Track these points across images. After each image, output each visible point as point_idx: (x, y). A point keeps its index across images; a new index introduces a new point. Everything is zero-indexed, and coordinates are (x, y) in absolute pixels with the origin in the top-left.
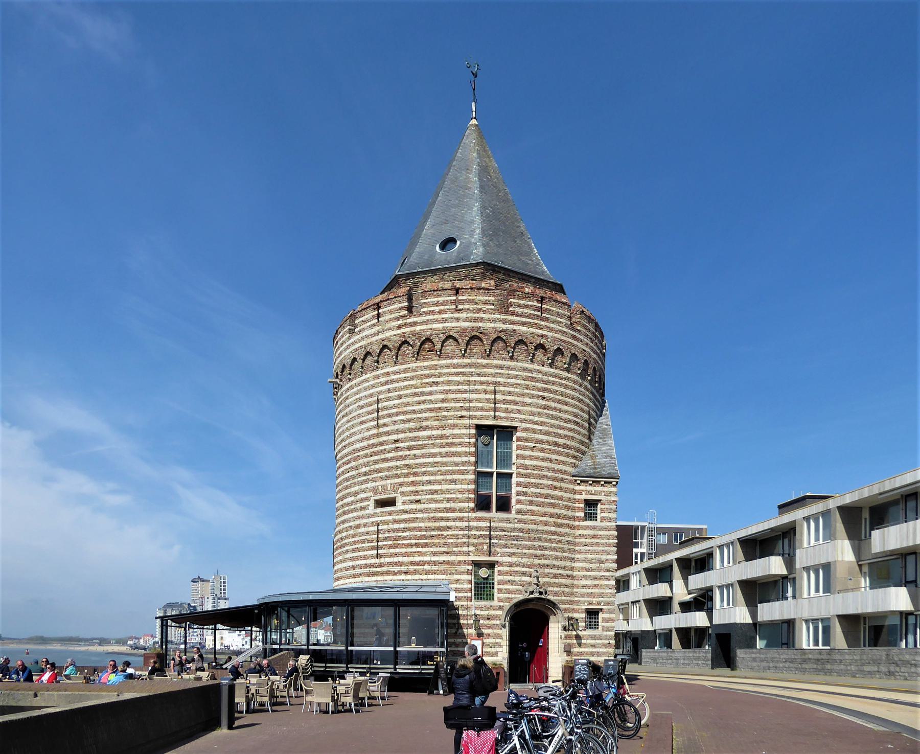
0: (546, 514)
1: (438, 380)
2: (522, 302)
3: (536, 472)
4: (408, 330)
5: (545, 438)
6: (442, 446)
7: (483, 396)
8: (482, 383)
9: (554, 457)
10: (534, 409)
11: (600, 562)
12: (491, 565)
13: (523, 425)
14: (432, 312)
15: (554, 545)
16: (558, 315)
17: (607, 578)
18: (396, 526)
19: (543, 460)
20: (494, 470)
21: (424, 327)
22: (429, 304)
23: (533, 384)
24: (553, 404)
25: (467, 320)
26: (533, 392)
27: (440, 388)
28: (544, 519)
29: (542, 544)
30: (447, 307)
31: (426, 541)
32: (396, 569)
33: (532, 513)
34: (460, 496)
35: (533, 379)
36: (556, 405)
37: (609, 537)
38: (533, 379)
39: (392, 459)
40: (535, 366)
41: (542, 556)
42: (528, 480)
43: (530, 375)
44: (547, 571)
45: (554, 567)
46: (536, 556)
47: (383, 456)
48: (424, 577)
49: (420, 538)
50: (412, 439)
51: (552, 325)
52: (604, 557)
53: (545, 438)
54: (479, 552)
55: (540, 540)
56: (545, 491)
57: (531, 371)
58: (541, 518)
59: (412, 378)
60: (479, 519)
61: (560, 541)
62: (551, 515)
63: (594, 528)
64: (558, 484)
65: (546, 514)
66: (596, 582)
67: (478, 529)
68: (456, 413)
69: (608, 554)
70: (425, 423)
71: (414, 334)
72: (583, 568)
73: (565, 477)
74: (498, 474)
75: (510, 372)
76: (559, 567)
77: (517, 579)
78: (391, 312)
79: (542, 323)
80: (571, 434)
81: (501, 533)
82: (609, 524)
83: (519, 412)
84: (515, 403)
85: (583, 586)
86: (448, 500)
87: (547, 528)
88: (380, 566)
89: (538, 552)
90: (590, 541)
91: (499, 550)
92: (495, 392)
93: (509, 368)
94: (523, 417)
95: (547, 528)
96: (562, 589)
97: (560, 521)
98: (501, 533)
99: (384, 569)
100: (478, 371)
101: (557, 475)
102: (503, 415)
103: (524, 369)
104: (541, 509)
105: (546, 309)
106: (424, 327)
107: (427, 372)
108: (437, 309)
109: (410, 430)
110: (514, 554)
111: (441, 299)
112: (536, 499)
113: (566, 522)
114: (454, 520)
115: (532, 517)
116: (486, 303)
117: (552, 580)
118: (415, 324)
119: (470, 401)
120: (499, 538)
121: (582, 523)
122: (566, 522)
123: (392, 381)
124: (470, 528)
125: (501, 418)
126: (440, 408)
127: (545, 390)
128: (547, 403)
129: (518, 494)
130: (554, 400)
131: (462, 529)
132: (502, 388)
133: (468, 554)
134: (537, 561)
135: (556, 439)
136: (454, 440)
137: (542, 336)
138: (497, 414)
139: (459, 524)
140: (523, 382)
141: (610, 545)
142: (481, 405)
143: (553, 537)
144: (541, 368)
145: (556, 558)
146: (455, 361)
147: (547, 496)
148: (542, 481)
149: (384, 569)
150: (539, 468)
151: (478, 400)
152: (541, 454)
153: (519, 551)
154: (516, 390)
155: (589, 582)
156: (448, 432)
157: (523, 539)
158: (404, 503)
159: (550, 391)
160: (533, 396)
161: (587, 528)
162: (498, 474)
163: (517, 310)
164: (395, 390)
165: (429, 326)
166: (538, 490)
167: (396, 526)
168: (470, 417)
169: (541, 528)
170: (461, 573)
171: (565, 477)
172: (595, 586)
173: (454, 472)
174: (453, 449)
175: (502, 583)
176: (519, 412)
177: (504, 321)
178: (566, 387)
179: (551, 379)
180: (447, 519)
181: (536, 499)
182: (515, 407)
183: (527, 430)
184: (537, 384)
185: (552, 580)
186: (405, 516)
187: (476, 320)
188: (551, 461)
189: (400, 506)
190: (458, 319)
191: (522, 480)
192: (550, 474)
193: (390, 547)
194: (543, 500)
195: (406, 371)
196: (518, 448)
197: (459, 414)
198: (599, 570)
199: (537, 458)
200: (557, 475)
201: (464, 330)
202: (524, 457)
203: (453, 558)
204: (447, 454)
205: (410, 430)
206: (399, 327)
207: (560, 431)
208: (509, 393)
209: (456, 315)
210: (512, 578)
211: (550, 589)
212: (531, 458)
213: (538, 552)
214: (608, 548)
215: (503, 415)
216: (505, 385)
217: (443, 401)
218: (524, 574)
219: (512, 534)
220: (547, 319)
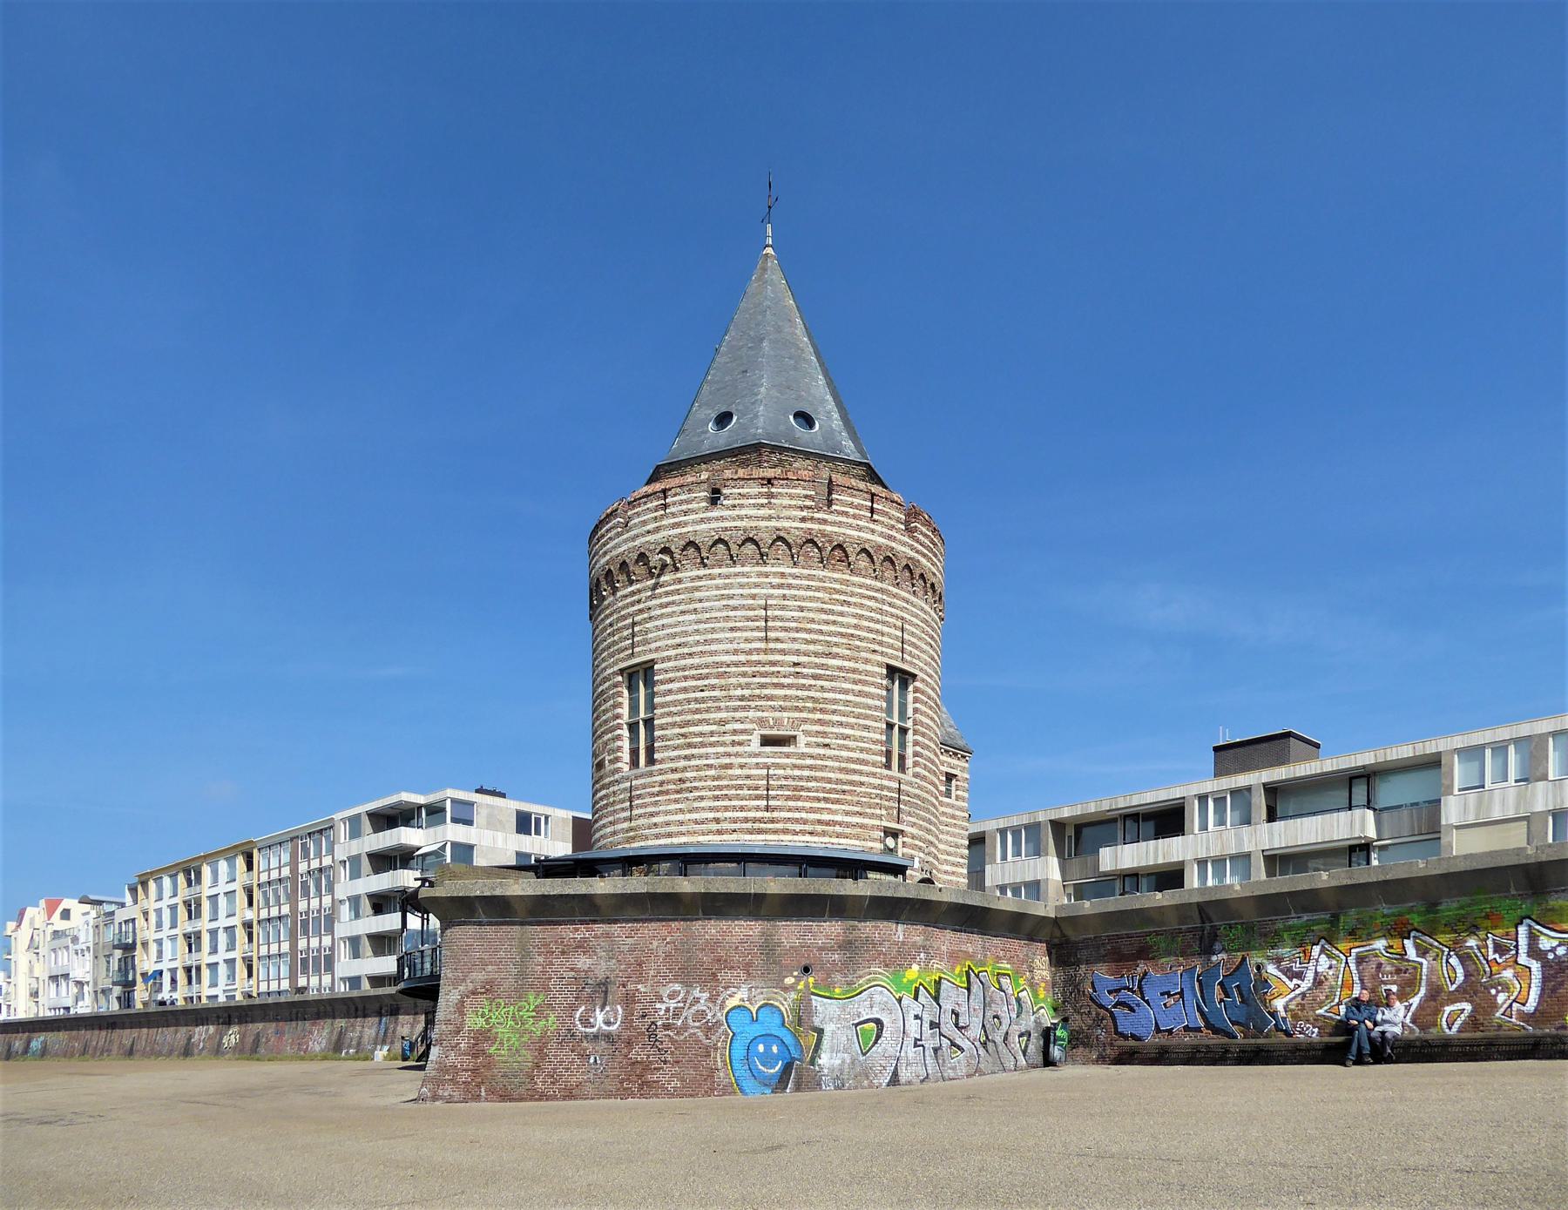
4: (816, 526)
14: (845, 514)
18: (797, 773)
21: (836, 529)
22: (843, 504)
32: (798, 827)
39: (790, 686)
47: (775, 680)
50: (817, 666)
59: (818, 589)
70: (835, 650)
78: (791, 497)
86: (862, 750)
88: (772, 821)
99: (780, 826)
106: (836, 529)
107: (837, 586)
108: (851, 511)
109: (816, 654)
114: (868, 775)
118: (825, 522)
123: (790, 586)
139: (872, 780)
149: (780, 826)
156: (861, 666)
158: (808, 745)
164: (794, 598)
165: (842, 530)
167: (797, 773)
170: (874, 840)
173: (867, 717)
174: (866, 689)
180: (861, 773)
186: (809, 762)
193: (788, 798)
195: (809, 578)
203: (866, 821)
204: (860, 694)
205: (816, 654)
206: (803, 520)
217: (856, 627)
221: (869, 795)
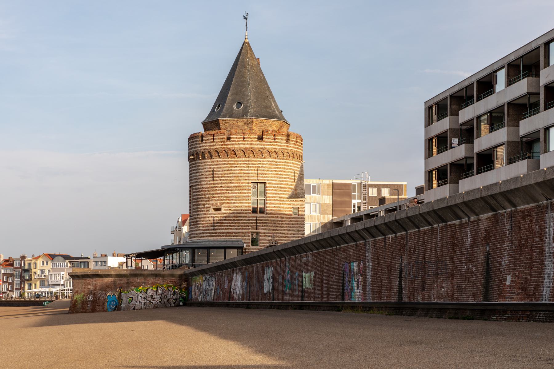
2: (268, 137)
4: (225, 146)
5: (277, 186)
6: (239, 190)
7: (253, 172)
8: (253, 167)
9: (280, 192)
11: (298, 231)
12: (257, 233)
19: (276, 194)
21: (232, 146)
24: (279, 173)
35: (271, 165)
36: (281, 173)
38: (271, 165)
39: (220, 193)
40: (273, 160)
45: (280, 233)
46: (274, 230)
49: (231, 223)
53: (277, 186)
54: (252, 229)
55: (275, 223)
67: (252, 220)
70: (233, 181)
76: (282, 233)
77: (267, 238)
83: (267, 177)
84: (266, 174)
93: (263, 161)
99: (217, 234)
103: (269, 161)
106: (232, 146)
108: (236, 140)
114: (244, 217)
116: (254, 138)
120: (259, 223)
124: (249, 220)
127: (276, 168)
130: (280, 171)
133: (249, 229)
137: (275, 149)
144: (275, 160)
145: (281, 230)
149: (217, 234)
150: (275, 197)
151: (252, 173)
152: (275, 192)
156: (241, 185)
157: (269, 223)
158: (224, 210)
159: (278, 168)
160: (272, 171)
168: (249, 180)
169: (275, 219)
173: (243, 200)
174: (243, 191)
176: (267, 177)
178: (284, 165)
180: (241, 217)
183: (269, 183)
187: (251, 144)
188: (279, 194)
190: (244, 144)
198: (298, 234)
199: (273, 194)
203: (243, 231)
204: (241, 193)
207: (282, 182)
208: (263, 170)
209: (244, 143)
217: (239, 173)
218: (269, 236)
220: (277, 142)
221: (244, 223)
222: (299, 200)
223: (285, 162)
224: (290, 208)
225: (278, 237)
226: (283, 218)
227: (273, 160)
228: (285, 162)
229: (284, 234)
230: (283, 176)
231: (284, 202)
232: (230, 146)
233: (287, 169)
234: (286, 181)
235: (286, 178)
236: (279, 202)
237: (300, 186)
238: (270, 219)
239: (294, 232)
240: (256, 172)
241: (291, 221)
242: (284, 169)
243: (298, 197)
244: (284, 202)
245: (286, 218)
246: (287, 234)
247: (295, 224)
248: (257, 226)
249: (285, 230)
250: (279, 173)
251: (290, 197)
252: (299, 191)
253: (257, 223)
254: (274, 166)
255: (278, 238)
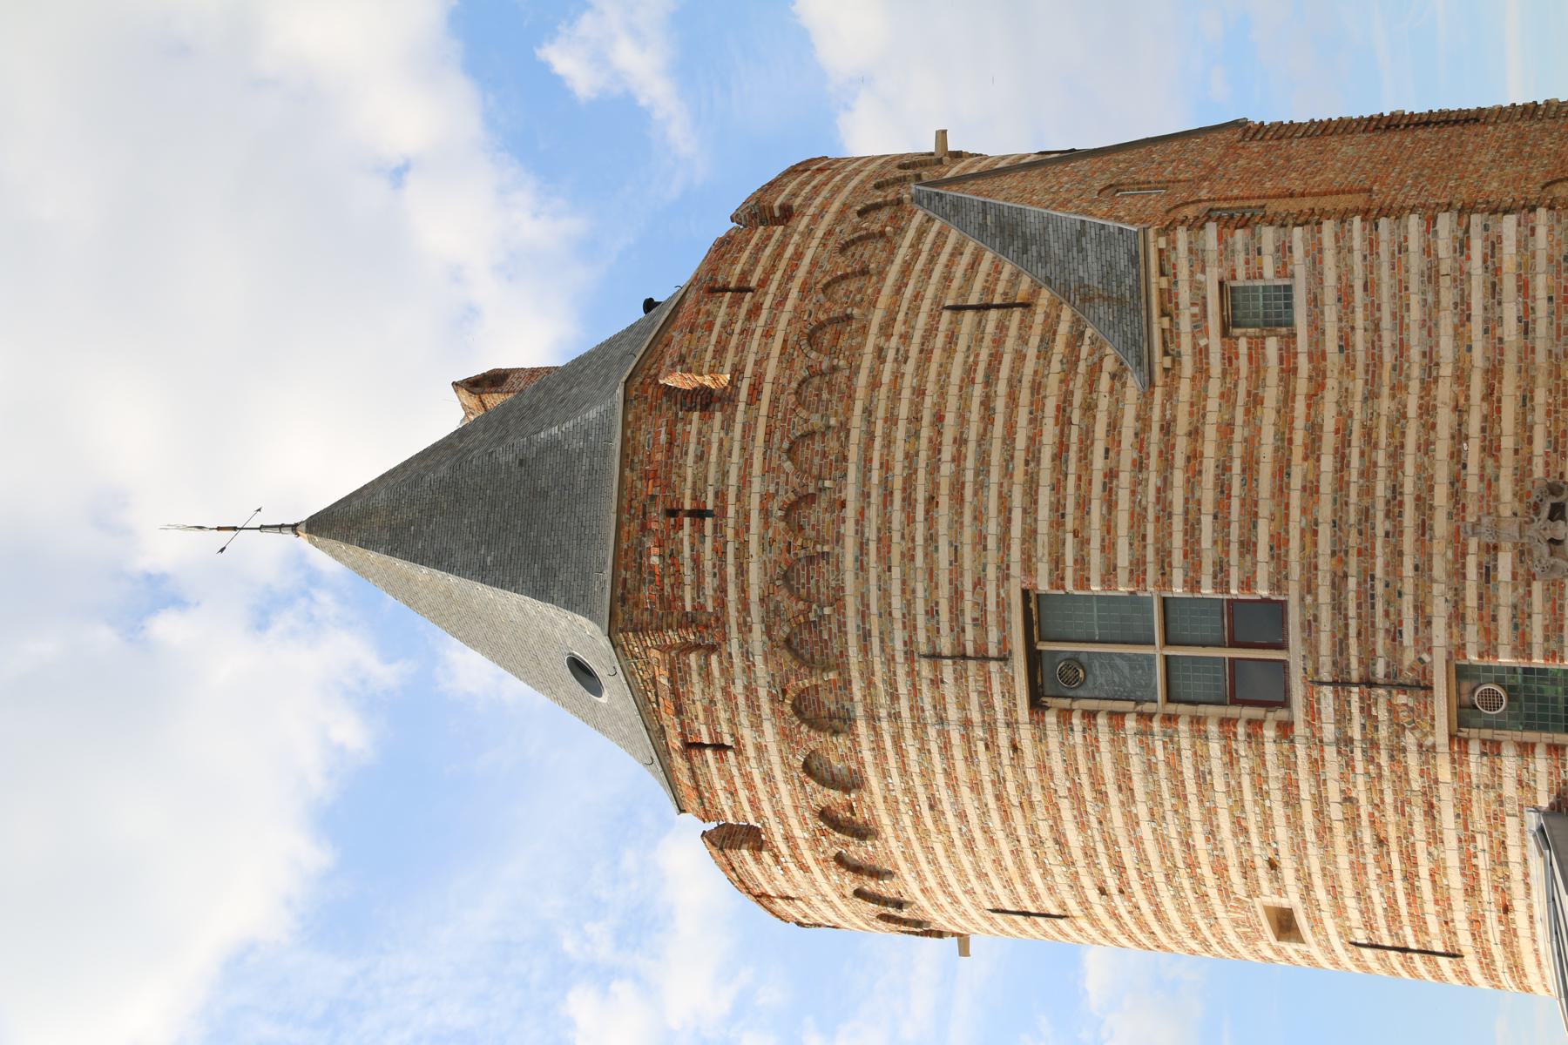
0: (1281, 490)
1: (922, 798)
2: (688, 575)
3: (1150, 529)
7: (949, 689)
8: (915, 691)
9: (1098, 463)
10: (968, 534)
11: (1432, 276)
12: (1461, 673)
13: (1016, 569)
15: (1381, 457)
16: (701, 457)
17: (1494, 246)
19: (1110, 504)
20: (1158, 652)
21: (794, 822)
23: (896, 537)
24: (946, 469)
25: (757, 726)
26: (920, 540)
27: (944, 795)
28: (1295, 499)
29: (1380, 506)
30: (735, 771)
31: (1395, 856)
33: (1279, 544)
34: (1245, 764)
35: (884, 542)
36: (947, 453)
37: (1343, 250)
38: (884, 542)
40: (849, 529)
41: (1423, 503)
42: (1177, 557)
43: (873, 547)
44: (1473, 485)
45: (1457, 456)
46: (1424, 528)
48: (1516, 872)
51: (733, 479)
52: (1415, 261)
54: (1420, 718)
55: (1366, 514)
56: (1208, 495)
57: (862, 546)
58: (1295, 513)
60: (1313, 712)
61: (1368, 433)
62: (1282, 471)
63: (1315, 301)
64: (1182, 445)
65: (1281, 490)
66: (1509, 284)
67: (1342, 718)
68: (1006, 761)
69: (1402, 249)
71: (815, 842)
72: (1457, 335)
73: (1156, 415)
74: (1167, 642)
75: (874, 609)
76: (1459, 436)
77: (1506, 596)
79: (731, 511)
80: (1025, 396)
81: (1354, 649)
82: (1298, 252)
83: (979, 583)
84: (957, 595)
85: (1526, 329)
87: (1326, 486)
89: (1409, 517)
90: (1359, 315)
91: (1409, 658)
92: (935, 656)
93: (864, 615)
94: (992, 573)
95: (1326, 486)
96: (1539, 416)
97: (1299, 437)
98: (1354, 649)
100: (883, 699)
101: (1154, 451)
102: (993, 635)
103: (861, 567)
104: (1264, 509)
105: (694, 498)
106: (794, 822)
108: (743, 794)
110: (1419, 608)
111: (719, 784)
112: (1235, 531)
113: (1300, 406)
115: (1294, 544)
117: (1507, 459)
119: (967, 723)
120: (1368, 659)
121: (1302, 343)
122: (1300, 406)
125: (1003, 641)
126: (998, 798)
127: (909, 501)
128: (944, 489)
129: (1221, 583)
130: (933, 469)
131: (1349, 764)
132: (921, 636)
134: (1441, 525)
135: (1047, 454)
136: (1083, 769)
137: (765, 513)
138: (993, 651)
140: (896, 572)
141: (1372, 244)
142: (974, 697)
143: (1355, 461)
144: (850, 512)
145: (1426, 447)
146: (867, 756)
147: (1223, 489)
148: (1178, 508)
150: (1137, 518)
152: (1096, 509)
153: (1408, 587)
154: (920, 593)
155: (1510, 312)
157: (1368, 576)
160: (931, 539)
161: (1316, 327)
162: (1167, 642)
163: (709, 591)
165: (790, 812)
166: (1207, 521)
168: (1011, 725)
169: (1325, 511)
171: (1156, 415)
172: (1524, 287)
175: (1523, 646)
176: (979, 583)
177: (745, 628)
178: (892, 420)
179: (875, 477)
181: (1235, 531)
182: (968, 596)
184: (896, 525)
185: (1507, 459)
187: (754, 707)
188: (1111, 475)
189: (1292, 900)
190: (760, 749)
191: (1178, 576)
192: (1154, 480)
194: (1235, 504)
196: (1083, 582)
197: (1006, 752)
198: (1461, 278)
199: (1109, 527)
200: (1154, 451)
201: (785, 736)
202: (1110, 572)
207: (1021, 442)
208: (932, 613)
210: (1504, 616)
211: (1538, 471)
212: (1108, 547)
213: (1409, 517)
214: (1384, 250)
215: (993, 635)
216: (909, 624)
217: (976, 787)
218: (1488, 573)
219: (1352, 612)
220: (720, 495)
222: (1157, 282)
223: (868, 412)
224: (1229, 359)
225: (1489, 482)
226: (1314, 429)
227: (849, 529)
228: (868, 412)
229: (1459, 410)
230: (973, 433)
231: (1182, 426)
232: (797, 832)
233: (919, 392)
234: (1013, 398)
235: (987, 404)
236: (1178, 477)
237: (1056, 248)
238: (1325, 563)
239: (1447, 321)
240: (948, 669)
241: (1345, 346)
242: (915, 419)
243: (1140, 290)
244: (1182, 426)
245: (1314, 398)
246: (1461, 377)
247: (1373, 307)
248: (1394, 683)
249: (1427, 410)
250: (946, 469)
251: (1144, 364)
252: (1090, 271)
253: (1369, 683)
254: (897, 517)
255: (1506, 487)
